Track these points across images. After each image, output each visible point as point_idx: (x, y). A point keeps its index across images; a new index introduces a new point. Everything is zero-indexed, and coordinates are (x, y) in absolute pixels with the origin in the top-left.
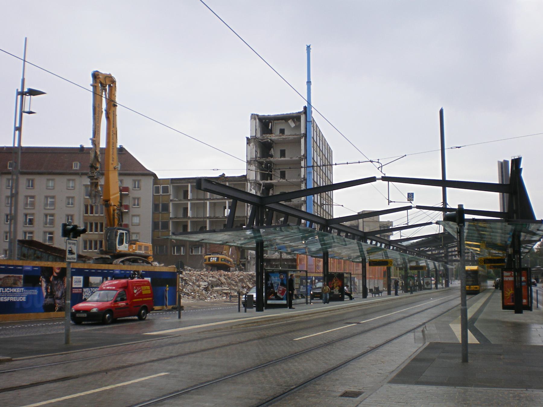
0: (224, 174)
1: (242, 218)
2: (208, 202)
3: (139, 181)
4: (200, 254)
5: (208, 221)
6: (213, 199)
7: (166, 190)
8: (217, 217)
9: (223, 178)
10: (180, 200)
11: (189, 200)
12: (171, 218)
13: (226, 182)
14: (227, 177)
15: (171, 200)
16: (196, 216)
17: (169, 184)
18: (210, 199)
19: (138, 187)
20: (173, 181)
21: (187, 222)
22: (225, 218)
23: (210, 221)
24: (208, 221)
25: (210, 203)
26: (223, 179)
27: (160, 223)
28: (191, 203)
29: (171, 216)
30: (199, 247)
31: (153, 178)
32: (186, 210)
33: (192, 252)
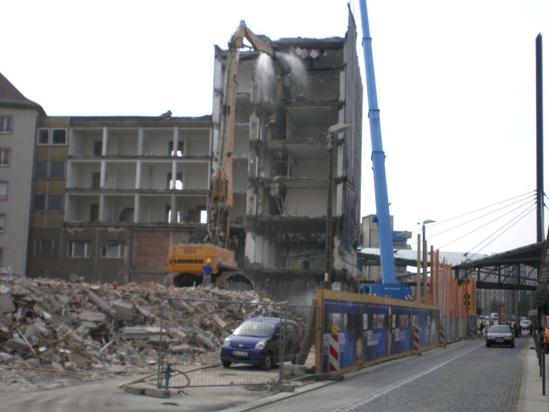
0: (170, 113)
1: (202, 194)
2: (139, 163)
3: (10, 118)
4: (119, 256)
5: (137, 197)
6: (149, 157)
7: (60, 137)
8: (154, 190)
9: (169, 118)
10: (86, 157)
11: (103, 158)
12: (67, 190)
13: (173, 126)
14: (176, 119)
15: (70, 157)
16: (115, 188)
17: (67, 127)
18: (143, 157)
19: (8, 129)
20: (74, 121)
21: (98, 197)
22: (169, 193)
23: (141, 199)
24: (137, 197)
25: (143, 165)
26: (168, 121)
27: (47, 198)
28: (108, 165)
29: (68, 185)
30: (117, 245)
31: (36, 113)
32: (97, 176)
33: (104, 253)
